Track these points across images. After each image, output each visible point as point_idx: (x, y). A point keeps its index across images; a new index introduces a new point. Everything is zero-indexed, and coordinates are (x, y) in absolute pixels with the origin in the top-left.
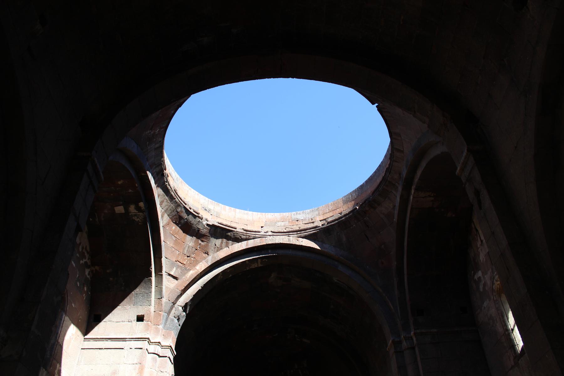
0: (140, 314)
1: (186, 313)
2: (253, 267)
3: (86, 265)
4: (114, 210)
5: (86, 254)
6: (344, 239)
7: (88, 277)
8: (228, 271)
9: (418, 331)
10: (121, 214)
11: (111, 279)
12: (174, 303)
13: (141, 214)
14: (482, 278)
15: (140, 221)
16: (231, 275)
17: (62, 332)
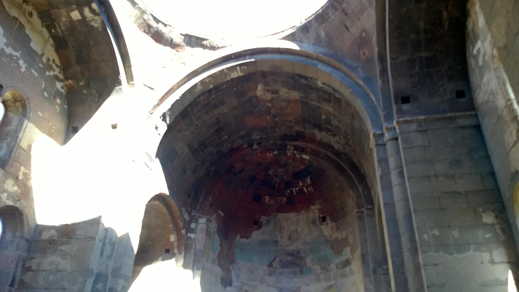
0: (114, 123)
1: (166, 122)
2: (234, 77)
3: (56, 77)
4: (71, 17)
5: (54, 66)
6: (323, 34)
7: (63, 91)
8: (207, 81)
9: (401, 119)
10: (79, 21)
11: (85, 91)
12: (151, 112)
13: (97, 17)
14: (482, 49)
15: (99, 26)
16: (211, 86)
17: (24, 137)
